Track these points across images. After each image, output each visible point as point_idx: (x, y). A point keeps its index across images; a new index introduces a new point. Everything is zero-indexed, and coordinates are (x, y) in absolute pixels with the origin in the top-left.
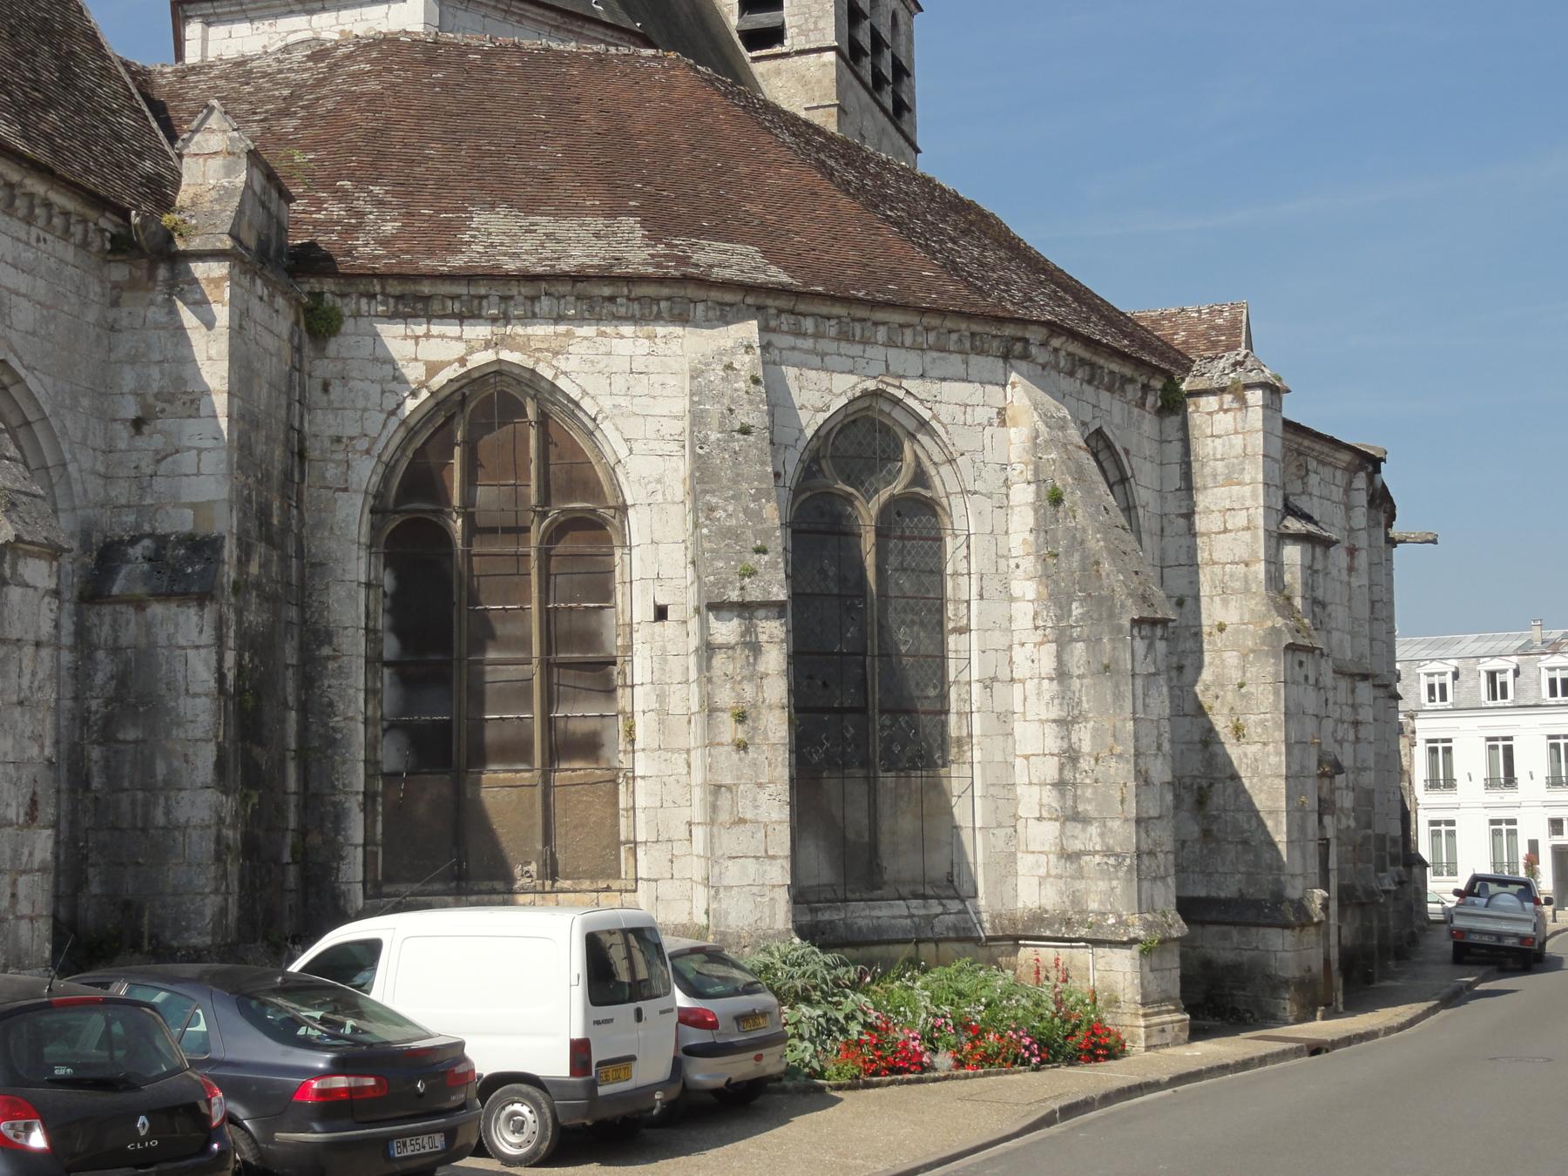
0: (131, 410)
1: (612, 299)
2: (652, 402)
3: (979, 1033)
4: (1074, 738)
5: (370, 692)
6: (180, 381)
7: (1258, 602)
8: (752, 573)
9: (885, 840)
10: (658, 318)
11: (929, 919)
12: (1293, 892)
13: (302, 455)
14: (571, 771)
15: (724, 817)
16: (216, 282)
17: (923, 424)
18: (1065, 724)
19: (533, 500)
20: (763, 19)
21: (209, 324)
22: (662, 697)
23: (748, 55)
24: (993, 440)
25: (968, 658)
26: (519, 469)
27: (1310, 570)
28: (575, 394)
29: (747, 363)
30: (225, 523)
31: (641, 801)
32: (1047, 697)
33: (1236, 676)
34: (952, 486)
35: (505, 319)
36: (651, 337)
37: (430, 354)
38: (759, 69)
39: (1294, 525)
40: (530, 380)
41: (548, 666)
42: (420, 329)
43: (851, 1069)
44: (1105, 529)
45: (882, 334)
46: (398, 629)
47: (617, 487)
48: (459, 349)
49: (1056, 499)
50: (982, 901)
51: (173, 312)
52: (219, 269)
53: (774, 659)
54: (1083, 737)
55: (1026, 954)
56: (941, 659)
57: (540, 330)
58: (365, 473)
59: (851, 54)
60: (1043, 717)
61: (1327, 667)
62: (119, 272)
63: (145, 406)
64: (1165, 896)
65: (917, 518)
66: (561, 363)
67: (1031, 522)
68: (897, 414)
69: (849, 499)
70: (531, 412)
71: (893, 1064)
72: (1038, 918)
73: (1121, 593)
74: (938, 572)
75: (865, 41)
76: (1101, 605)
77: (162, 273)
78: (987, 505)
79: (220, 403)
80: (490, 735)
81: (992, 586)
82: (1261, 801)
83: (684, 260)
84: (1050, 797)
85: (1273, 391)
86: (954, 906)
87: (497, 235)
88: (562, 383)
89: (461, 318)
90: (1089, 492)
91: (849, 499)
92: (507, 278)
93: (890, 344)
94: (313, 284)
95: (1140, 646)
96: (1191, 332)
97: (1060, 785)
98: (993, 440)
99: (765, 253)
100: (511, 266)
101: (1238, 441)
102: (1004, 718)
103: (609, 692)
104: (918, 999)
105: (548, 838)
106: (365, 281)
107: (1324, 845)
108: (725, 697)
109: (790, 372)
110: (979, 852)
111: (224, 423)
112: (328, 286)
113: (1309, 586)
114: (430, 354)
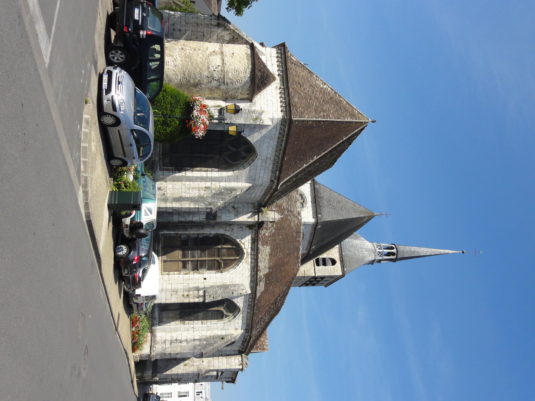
0: (236, 206)
2: (237, 278)
3: (137, 333)
5: (194, 234)
6: (240, 213)
7: (207, 368)
8: (210, 296)
9: (169, 312)
10: (251, 278)
11: (155, 319)
12: (158, 375)
13: (230, 225)
14: (181, 264)
15: (172, 293)
16: (254, 219)
17: (235, 317)
18: (186, 341)
19: (223, 258)
20: (321, 262)
21: (248, 218)
22: (192, 279)
23: (314, 259)
24: (233, 328)
25: (197, 324)
26: (228, 256)
27: (212, 376)
29: (244, 292)
30: (218, 220)
31: (175, 276)
33: (195, 364)
34: (225, 321)
35: (251, 255)
37: (246, 243)
38: (312, 261)
39: (220, 373)
40: (241, 258)
41: (197, 261)
42: (250, 242)
43: (133, 318)
44: (218, 347)
45: (249, 311)
46: (204, 237)
47: (225, 271)
48: (247, 248)
49: (223, 339)
50: (158, 327)
51: (250, 212)
52: (256, 219)
53: (197, 300)
54: (184, 344)
55: (149, 334)
56: (198, 320)
57: (249, 260)
58: (228, 233)
59: (315, 278)
61: (197, 379)
62: (256, 204)
63: (236, 208)
64: (158, 357)
65: (220, 316)
66: (244, 263)
67: (219, 334)
68: (237, 313)
69: (223, 306)
70: (237, 258)
71: (133, 323)
72: (155, 336)
73: (207, 350)
74: (211, 319)
75: (318, 280)
76: (205, 347)
77: (256, 211)
78: (222, 327)
79: (236, 220)
80: (186, 252)
81: (209, 328)
82: (173, 369)
83: (260, 281)
84: (175, 338)
85: (242, 370)
86: (157, 323)
87: (265, 251)
89: (252, 248)
90: (224, 344)
91: (223, 306)
92: (257, 255)
94: (257, 226)
95: (199, 353)
96: (263, 341)
97: (177, 340)
98: (233, 328)
99: (263, 292)
100: (259, 255)
101: (234, 364)
102: (188, 330)
103: (193, 270)
104: (144, 323)
105: (170, 261)
106: (257, 234)
107: (166, 379)
108: (191, 293)
109: (243, 297)
110: (166, 326)
111: (233, 220)
112: (256, 228)
113: (210, 376)
114: (246, 243)
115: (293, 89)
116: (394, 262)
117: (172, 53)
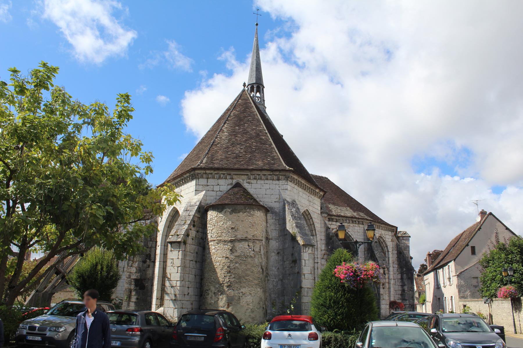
17: (384, 241)
48: (335, 227)
84: (399, 296)
92: (342, 216)
93: (382, 229)
115: (248, 165)
117: (236, 298)
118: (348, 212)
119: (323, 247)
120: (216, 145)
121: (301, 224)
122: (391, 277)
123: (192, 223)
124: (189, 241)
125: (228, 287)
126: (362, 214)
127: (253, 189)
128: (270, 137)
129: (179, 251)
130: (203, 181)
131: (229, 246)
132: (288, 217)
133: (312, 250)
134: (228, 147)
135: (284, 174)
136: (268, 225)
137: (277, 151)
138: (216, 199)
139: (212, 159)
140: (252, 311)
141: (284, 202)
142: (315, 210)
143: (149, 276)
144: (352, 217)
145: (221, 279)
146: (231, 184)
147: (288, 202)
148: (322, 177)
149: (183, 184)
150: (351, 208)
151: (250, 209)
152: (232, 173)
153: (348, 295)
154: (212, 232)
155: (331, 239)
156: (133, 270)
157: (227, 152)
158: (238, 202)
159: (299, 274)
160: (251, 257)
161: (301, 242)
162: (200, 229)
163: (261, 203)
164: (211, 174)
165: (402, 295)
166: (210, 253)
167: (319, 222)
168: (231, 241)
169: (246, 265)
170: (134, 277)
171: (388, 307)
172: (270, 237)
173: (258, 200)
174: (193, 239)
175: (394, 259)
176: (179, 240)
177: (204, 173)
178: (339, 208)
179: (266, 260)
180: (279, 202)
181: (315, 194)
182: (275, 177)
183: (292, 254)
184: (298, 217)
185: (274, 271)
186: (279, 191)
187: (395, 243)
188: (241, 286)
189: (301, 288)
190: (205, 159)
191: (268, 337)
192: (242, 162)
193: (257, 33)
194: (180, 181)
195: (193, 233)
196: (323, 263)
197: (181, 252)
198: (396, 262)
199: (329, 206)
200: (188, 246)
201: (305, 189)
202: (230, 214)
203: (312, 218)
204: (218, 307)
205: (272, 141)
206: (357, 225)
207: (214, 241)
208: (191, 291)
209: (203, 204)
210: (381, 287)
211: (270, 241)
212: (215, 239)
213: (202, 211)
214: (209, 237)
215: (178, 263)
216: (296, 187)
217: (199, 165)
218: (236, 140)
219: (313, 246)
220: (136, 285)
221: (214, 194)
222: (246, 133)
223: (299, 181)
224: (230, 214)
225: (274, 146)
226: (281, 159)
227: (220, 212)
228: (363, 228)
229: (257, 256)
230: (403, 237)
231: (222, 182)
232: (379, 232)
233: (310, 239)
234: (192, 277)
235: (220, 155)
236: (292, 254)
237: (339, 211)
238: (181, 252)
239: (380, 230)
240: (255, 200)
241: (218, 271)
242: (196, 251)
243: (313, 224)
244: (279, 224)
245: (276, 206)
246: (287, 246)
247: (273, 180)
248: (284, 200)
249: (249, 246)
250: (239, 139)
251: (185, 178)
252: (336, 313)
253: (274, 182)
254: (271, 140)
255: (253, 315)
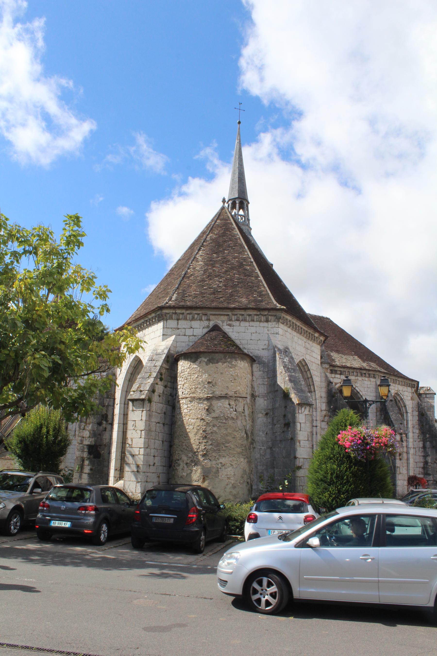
1: (365, 374)
4: (427, 459)
17: (402, 399)
28: (359, 391)
32: (421, 451)
34: (404, 411)
36: (370, 381)
48: (340, 381)
60: (420, 455)
67: (417, 418)
84: (421, 470)
88: (356, 388)
92: (348, 367)
93: (399, 384)
115: (228, 303)
116: (249, 203)
117: (214, 470)
118: (355, 362)
119: (324, 407)
120: (188, 277)
121: (295, 377)
122: (411, 445)
123: (159, 376)
124: (155, 398)
125: (204, 455)
126: (374, 365)
127: (233, 333)
128: (256, 267)
129: (143, 411)
130: (172, 323)
131: (205, 405)
132: (280, 369)
133: (309, 411)
134: (203, 280)
135: (274, 314)
136: (254, 379)
137: (265, 285)
138: (188, 345)
139: (183, 296)
140: (234, 487)
141: (274, 350)
142: (313, 360)
143: (105, 441)
144: (361, 369)
145: (195, 447)
146: (208, 327)
147: (279, 349)
148: (323, 318)
149: (148, 326)
150: (360, 357)
151: (231, 358)
152: (209, 312)
153: (354, 469)
154: (183, 388)
155: (333, 396)
156: (86, 434)
157: (203, 286)
158: (216, 349)
159: (293, 440)
160: (233, 418)
161: (295, 399)
162: (169, 384)
163: (246, 351)
164: (183, 314)
165: (424, 468)
166: (181, 413)
167: (319, 374)
168: (208, 399)
169: (226, 429)
170: (87, 442)
171: (406, 483)
172: (257, 394)
173: (241, 346)
174: (160, 396)
175: (415, 422)
176: (143, 397)
177: (173, 313)
178: (344, 357)
179: (251, 423)
180: (268, 350)
181: (314, 339)
182: (263, 318)
183: (285, 416)
184: (292, 369)
185: (261, 436)
186: (268, 336)
187: (415, 402)
188: (219, 455)
189: (295, 458)
190: (175, 295)
191: (254, 520)
192: (222, 299)
193: (239, 134)
194: (144, 323)
195: (160, 388)
196: (323, 427)
197: (144, 412)
198: (417, 426)
199: (332, 354)
200: (153, 404)
201: (301, 333)
202: (207, 365)
203: (309, 370)
204: (191, 481)
205: (259, 273)
206: (367, 379)
207: (186, 398)
208: (157, 460)
209: (172, 352)
210: (398, 457)
211: (257, 398)
212: (188, 396)
213: (172, 360)
214: (180, 393)
215: (141, 425)
216: (289, 330)
217: (167, 303)
218: (214, 271)
219: (310, 405)
220: (90, 453)
221: (186, 339)
222: (226, 262)
223: (293, 323)
224: (207, 365)
225: (261, 278)
226: (270, 295)
227: (194, 362)
228: (374, 383)
229: (240, 418)
230: (426, 394)
231: (196, 324)
232: (395, 388)
233: (306, 397)
234: (158, 444)
235: (193, 290)
236: (285, 416)
237: (344, 361)
238: (144, 412)
239: (397, 386)
240: (237, 347)
241: (191, 435)
242: (164, 410)
243: (311, 377)
244: (268, 378)
245: (265, 354)
246: (277, 405)
247: (260, 321)
248: (275, 347)
249: (229, 405)
250: (217, 270)
251: (150, 319)
252: (339, 491)
253: (262, 324)
254: (258, 271)
255: (234, 492)
